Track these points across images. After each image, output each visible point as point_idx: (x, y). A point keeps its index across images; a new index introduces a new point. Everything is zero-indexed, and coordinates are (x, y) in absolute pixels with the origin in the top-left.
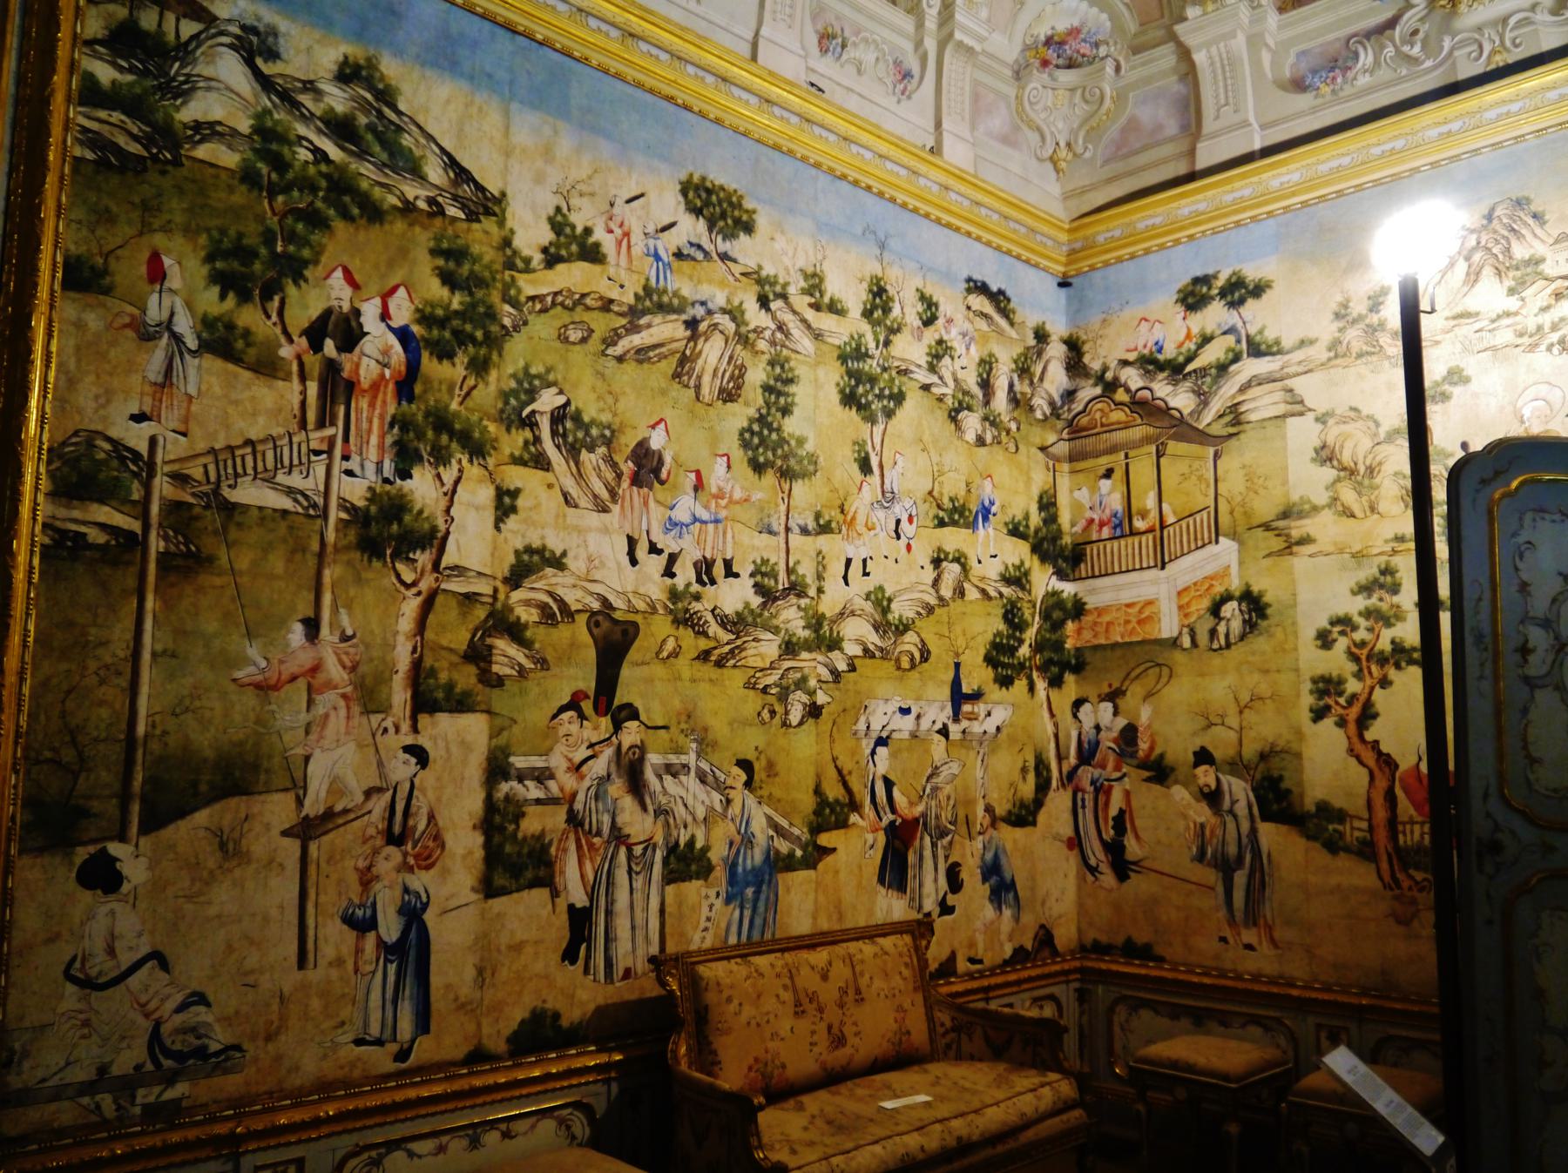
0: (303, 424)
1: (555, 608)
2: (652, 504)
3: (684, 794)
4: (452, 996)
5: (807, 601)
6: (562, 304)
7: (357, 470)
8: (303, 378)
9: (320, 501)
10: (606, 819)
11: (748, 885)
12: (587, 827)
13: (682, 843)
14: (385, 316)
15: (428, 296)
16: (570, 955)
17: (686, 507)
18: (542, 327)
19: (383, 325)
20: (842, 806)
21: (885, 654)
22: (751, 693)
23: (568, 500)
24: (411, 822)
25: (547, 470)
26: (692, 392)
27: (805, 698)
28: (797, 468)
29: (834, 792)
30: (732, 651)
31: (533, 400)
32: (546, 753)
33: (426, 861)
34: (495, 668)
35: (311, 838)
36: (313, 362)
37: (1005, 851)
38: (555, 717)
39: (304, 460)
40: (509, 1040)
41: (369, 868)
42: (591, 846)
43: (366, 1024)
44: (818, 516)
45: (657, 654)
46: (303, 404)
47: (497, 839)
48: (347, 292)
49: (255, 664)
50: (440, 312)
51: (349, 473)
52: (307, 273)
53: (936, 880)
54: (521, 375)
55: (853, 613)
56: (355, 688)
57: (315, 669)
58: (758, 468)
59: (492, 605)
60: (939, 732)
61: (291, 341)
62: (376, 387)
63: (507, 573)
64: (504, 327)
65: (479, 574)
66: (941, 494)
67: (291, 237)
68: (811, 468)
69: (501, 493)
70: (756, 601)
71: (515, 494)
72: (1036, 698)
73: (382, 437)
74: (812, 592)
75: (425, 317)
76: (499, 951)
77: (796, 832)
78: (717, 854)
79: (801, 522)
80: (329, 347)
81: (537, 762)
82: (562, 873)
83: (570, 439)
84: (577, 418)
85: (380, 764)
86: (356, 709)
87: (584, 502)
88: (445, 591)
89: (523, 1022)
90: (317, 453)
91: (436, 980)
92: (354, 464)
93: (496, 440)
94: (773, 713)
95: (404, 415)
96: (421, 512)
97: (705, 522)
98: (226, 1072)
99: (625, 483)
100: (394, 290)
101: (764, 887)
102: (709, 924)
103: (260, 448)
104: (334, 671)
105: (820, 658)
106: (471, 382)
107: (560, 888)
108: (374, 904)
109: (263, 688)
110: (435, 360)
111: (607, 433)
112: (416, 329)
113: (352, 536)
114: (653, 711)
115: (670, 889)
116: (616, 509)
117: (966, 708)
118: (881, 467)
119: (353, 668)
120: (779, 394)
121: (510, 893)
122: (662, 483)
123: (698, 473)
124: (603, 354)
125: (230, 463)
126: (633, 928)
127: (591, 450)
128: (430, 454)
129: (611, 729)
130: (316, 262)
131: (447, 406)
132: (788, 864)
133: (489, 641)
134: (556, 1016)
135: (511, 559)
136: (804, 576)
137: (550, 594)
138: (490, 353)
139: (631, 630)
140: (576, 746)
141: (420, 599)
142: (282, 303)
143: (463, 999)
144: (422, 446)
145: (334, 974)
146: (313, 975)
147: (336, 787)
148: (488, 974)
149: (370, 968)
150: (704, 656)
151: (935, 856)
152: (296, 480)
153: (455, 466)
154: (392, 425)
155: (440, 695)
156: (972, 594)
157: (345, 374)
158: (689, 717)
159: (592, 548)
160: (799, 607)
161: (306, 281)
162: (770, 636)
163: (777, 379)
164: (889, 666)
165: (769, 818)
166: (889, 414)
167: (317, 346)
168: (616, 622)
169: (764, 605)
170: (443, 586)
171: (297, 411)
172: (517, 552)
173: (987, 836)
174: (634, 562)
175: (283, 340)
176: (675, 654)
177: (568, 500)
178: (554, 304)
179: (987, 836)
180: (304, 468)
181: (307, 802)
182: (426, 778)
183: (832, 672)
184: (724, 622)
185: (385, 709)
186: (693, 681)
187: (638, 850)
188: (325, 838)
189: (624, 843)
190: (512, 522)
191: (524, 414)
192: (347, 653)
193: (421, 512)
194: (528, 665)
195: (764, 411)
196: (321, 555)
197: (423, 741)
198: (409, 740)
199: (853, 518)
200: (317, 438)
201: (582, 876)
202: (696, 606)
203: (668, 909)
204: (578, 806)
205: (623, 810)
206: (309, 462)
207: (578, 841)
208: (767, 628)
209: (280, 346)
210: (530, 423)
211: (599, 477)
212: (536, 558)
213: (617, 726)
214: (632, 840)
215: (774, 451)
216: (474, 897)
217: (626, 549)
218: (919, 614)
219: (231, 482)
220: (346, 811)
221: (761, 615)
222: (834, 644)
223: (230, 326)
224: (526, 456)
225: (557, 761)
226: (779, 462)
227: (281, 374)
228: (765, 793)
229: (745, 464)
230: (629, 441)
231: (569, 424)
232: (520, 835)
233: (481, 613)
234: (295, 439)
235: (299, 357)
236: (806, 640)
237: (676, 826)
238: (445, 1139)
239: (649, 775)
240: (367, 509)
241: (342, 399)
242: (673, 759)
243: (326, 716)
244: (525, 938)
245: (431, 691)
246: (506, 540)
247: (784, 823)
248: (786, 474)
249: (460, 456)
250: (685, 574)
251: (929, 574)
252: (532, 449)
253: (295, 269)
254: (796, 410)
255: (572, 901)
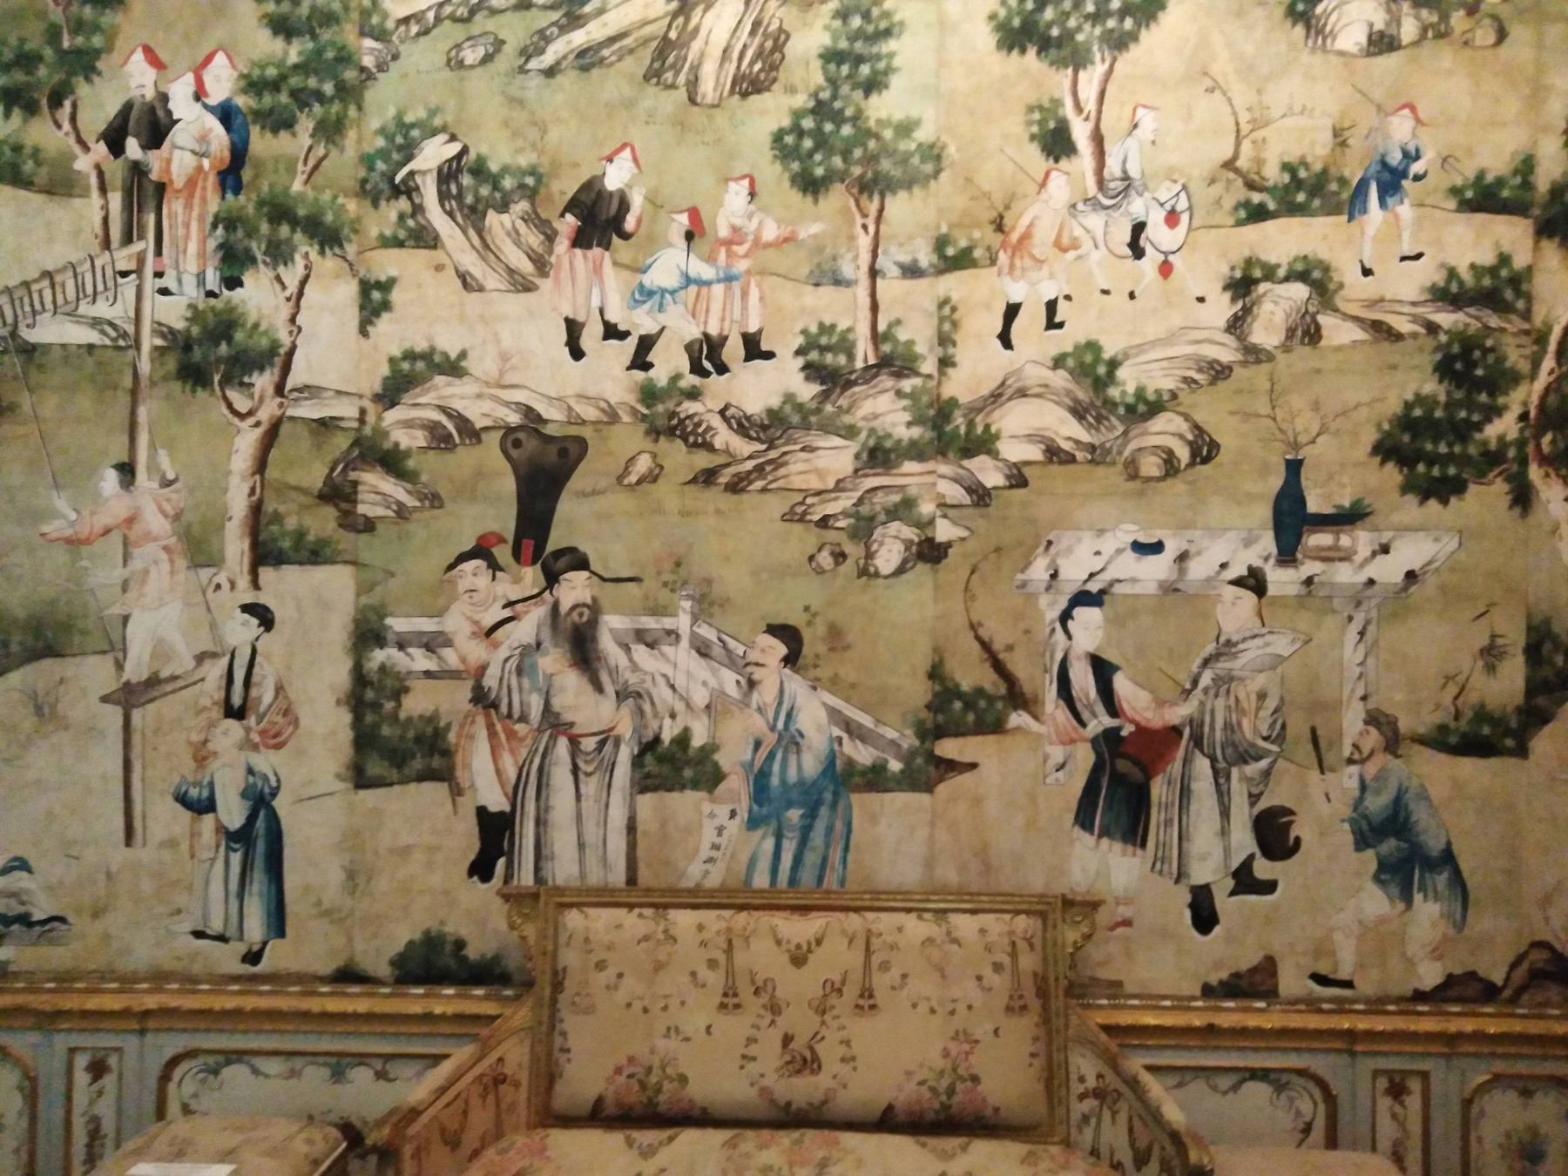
0: (106, 244)
1: (451, 427)
2: (607, 267)
3: (669, 671)
4: (313, 899)
5: (917, 381)
6: (455, 19)
7: (173, 286)
8: (103, 190)
9: (130, 329)
10: (536, 704)
11: (790, 804)
12: (504, 709)
13: (666, 737)
14: (199, 95)
15: (256, 55)
16: (481, 869)
17: (669, 264)
18: (422, 57)
19: (199, 105)
20: (991, 700)
21: (1098, 455)
22: (797, 528)
23: (467, 282)
24: (254, 693)
25: (435, 247)
26: (682, 94)
27: (910, 533)
28: (896, 173)
29: (971, 674)
30: (759, 469)
31: (409, 158)
32: (439, 613)
33: (273, 738)
34: (362, 509)
35: (134, 706)
36: (116, 170)
37: (1423, 796)
38: (451, 567)
39: (110, 284)
40: (393, 963)
41: (206, 741)
42: (511, 735)
43: (206, 917)
44: (941, 244)
45: (620, 479)
46: (106, 220)
47: (369, 718)
48: (150, 74)
49: (64, 517)
50: (272, 72)
51: (164, 292)
52: (100, 65)
53: (1224, 832)
54: (392, 128)
55: (1022, 393)
56: (180, 539)
57: (130, 521)
58: (810, 185)
59: (358, 430)
60: (1238, 582)
61: (86, 148)
62: (191, 183)
63: (378, 388)
64: (363, 69)
65: (339, 393)
66: (1260, 162)
67: (79, 27)
68: (928, 168)
69: (366, 287)
70: (807, 391)
71: (386, 286)
72: (1537, 515)
73: (203, 241)
74: (929, 366)
75: (254, 85)
76: (376, 853)
77: (891, 734)
78: (733, 756)
79: (905, 258)
80: (133, 147)
81: (427, 625)
82: (467, 766)
83: (469, 200)
84: (479, 171)
85: (213, 626)
86: (181, 563)
87: (492, 280)
88: (292, 418)
89: (411, 943)
90: (124, 274)
91: (291, 880)
92: (169, 281)
93: (358, 220)
94: (839, 557)
95: (229, 211)
96: (256, 326)
97: (708, 283)
98: (52, 943)
99: (562, 245)
100: (208, 59)
101: (824, 811)
102: (714, 854)
103: (58, 279)
104: (155, 522)
105: (944, 469)
106: (321, 151)
107: (465, 783)
108: (211, 785)
109: (74, 543)
110: (269, 135)
111: (530, 181)
112: (241, 101)
113: (171, 364)
114: (609, 553)
115: (646, 802)
116: (546, 285)
117: (1318, 539)
118: (1098, 139)
119: (177, 517)
120: (859, 60)
121: (391, 784)
122: (625, 236)
123: (694, 214)
124: (522, 70)
125: (26, 300)
126: (581, 846)
127: (503, 207)
128: (265, 254)
129: (543, 583)
130: (109, 48)
131: (287, 188)
132: (875, 779)
133: (353, 475)
134: (460, 944)
135: (385, 370)
136: (910, 343)
137: (444, 410)
138: (346, 109)
139: (573, 450)
140: (485, 605)
141: (259, 431)
142: (74, 106)
143: (326, 904)
144: (254, 245)
145: (167, 855)
146: (142, 854)
147: (161, 651)
148: (361, 880)
149: (212, 855)
150: (707, 477)
151: (1223, 795)
152: (102, 309)
153: (300, 262)
154: (214, 226)
155: (286, 544)
156: (1338, 332)
157: (154, 176)
158: (678, 564)
159: (507, 341)
160: (899, 394)
161: (99, 74)
162: (837, 441)
163: (853, 38)
164: (1111, 476)
165: (834, 714)
166: (1119, 43)
167: (116, 148)
168: (549, 439)
169: (825, 396)
170: (289, 412)
171: (99, 230)
172: (392, 361)
173: (1371, 769)
174: (577, 353)
175: (77, 149)
176: (652, 477)
177: (467, 282)
178: (438, 20)
179: (1371, 769)
180: (111, 294)
181: (128, 666)
182: (267, 642)
183: (969, 490)
184: (743, 426)
185: (216, 561)
186: (685, 513)
187: (589, 744)
188: (150, 707)
189: (564, 733)
190: (384, 325)
191: (398, 179)
192: (168, 500)
193: (256, 326)
194: (411, 502)
195: (825, 95)
196: (134, 392)
197: (264, 598)
198: (249, 598)
199: (1026, 236)
200: (124, 258)
201: (498, 772)
202: (690, 407)
203: (640, 828)
204: (490, 681)
205: (562, 689)
206: (116, 285)
207: (490, 727)
208: (827, 428)
209: (75, 157)
210: (407, 189)
211: (518, 244)
212: (420, 365)
213: (552, 579)
214: (575, 731)
215: (846, 155)
216: (340, 786)
217: (564, 337)
218: (1188, 381)
219: (30, 321)
220: (174, 678)
221: (818, 411)
222: (982, 444)
223: (17, 149)
224: (402, 234)
225: (456, 622)
226: (857, 171)
227: (77, 191)
228: (824, 673)
229: (786, 183)
230: (566, 186)
231: (466, 180)
232: (403, 715)
233: (342, 442)
234: (98, 263)
235: (98, 167)
236: (913, 443)
237: (656, 714)
238: (298, 1063)
239: (607, 644)
240: (188, 330)
241: (151, 204)
242: (649, 622)
243: (146, 572)
244: (411, 841)
245: (275, 540)
246: (375, 348)
247: (866, 720)
248: (873, 186)
249: (305, 248)
250: (669, 362)
251: (1222, 308)
252: (411, 223)
253: (84, 63)
254: (895, 81)
255: (482, 803)
